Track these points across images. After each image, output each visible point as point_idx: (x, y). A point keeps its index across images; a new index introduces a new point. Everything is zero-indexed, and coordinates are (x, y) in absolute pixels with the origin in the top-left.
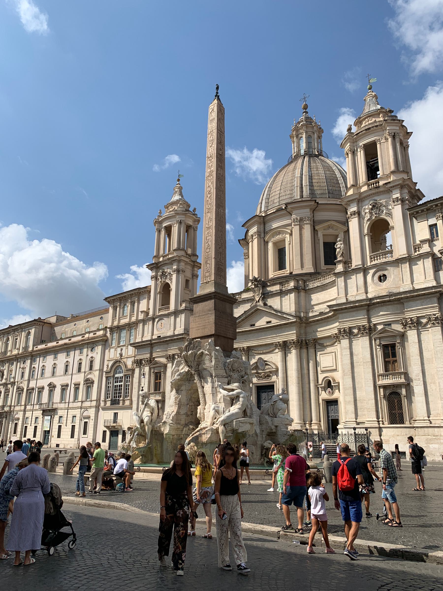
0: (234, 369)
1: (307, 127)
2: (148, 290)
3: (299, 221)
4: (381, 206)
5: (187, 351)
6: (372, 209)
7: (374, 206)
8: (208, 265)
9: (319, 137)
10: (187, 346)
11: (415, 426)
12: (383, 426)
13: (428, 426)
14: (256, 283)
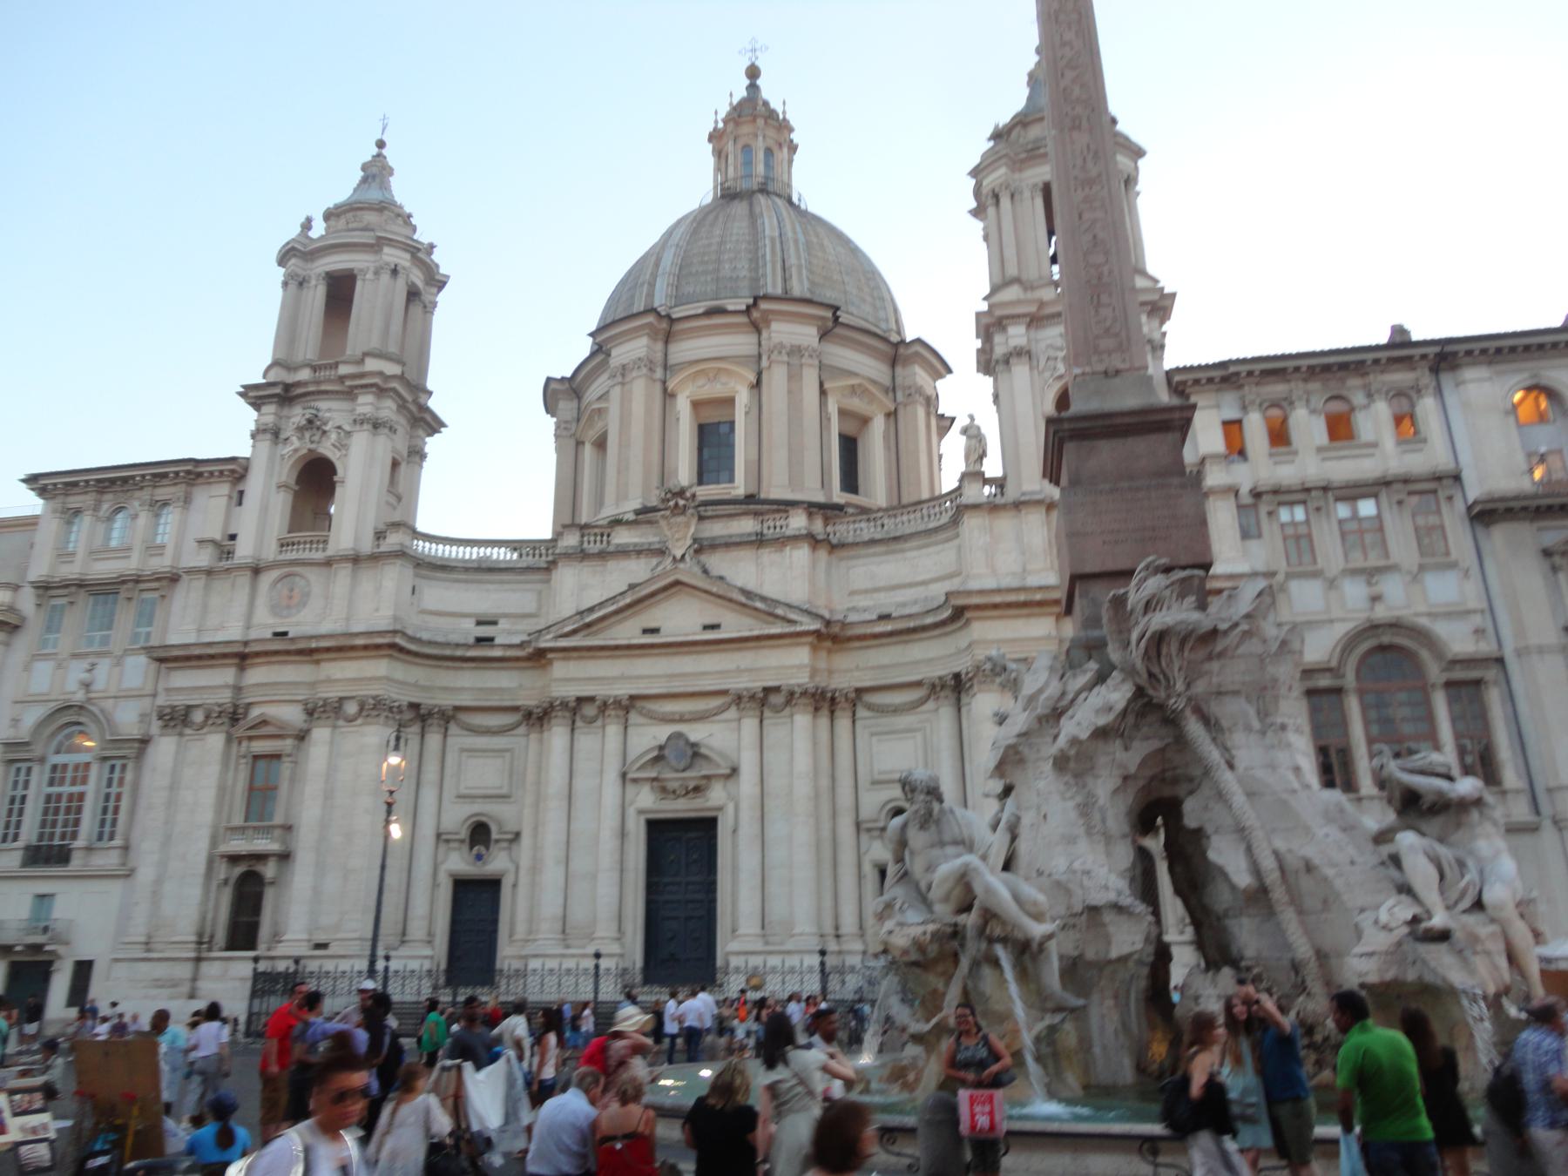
1: (766, 123)
2: (233, 471)
3: (788, 354)
8: (1105, 312)
9: (790, 162)
14: (681, 502)
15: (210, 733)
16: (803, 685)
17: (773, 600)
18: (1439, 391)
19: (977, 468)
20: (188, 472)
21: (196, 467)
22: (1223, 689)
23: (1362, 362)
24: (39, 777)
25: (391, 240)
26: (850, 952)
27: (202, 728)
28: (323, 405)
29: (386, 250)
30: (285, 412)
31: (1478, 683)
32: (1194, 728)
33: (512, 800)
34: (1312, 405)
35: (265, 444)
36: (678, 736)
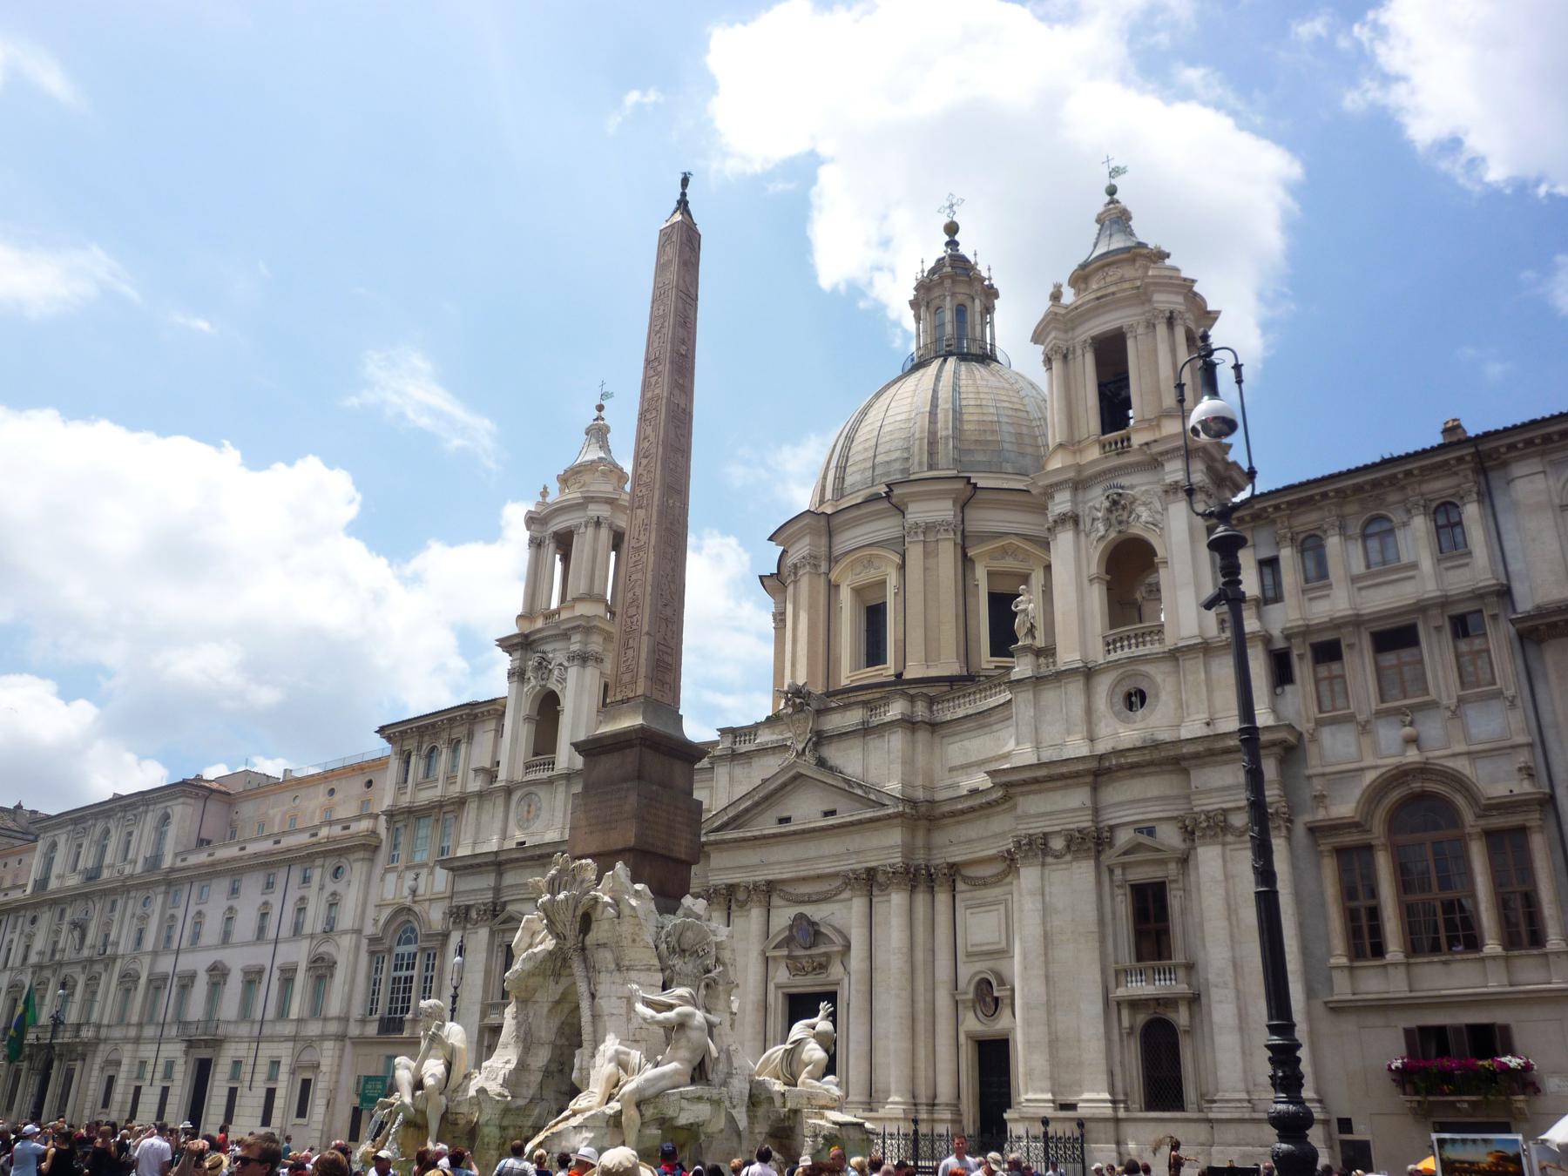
0: (686, 947)
1: (954, 282)
2: (496, 710)
3: (924, 533)
4: (1132, 503)
5: (553, 893)
6: (1109, 510)
7: (1115, 503)
8: (630, 652)
9: (989, 309)
10: (553, 879)
11: (1211, 1115)
12: (1122, 1114)
13: (1247, 1116)
14: (798, 701)
15: (481, 927)
16: (894, 865)
18: (1486, 497)
19: (1028, 641)
20: (468, 715)
21: (472, 709)
22: (600, 942)
23: (1394, 476)
24: (388, 965)
25: (593, 497)
26: (942, 1121)
27: (477, 923)
28: (548, 648)
29: (591, 506)
30: (530, 654)
31: (1523, 830)
32: (577, 967)
34: (1349, 533)
35: (515, 684)
36: (801, 916)
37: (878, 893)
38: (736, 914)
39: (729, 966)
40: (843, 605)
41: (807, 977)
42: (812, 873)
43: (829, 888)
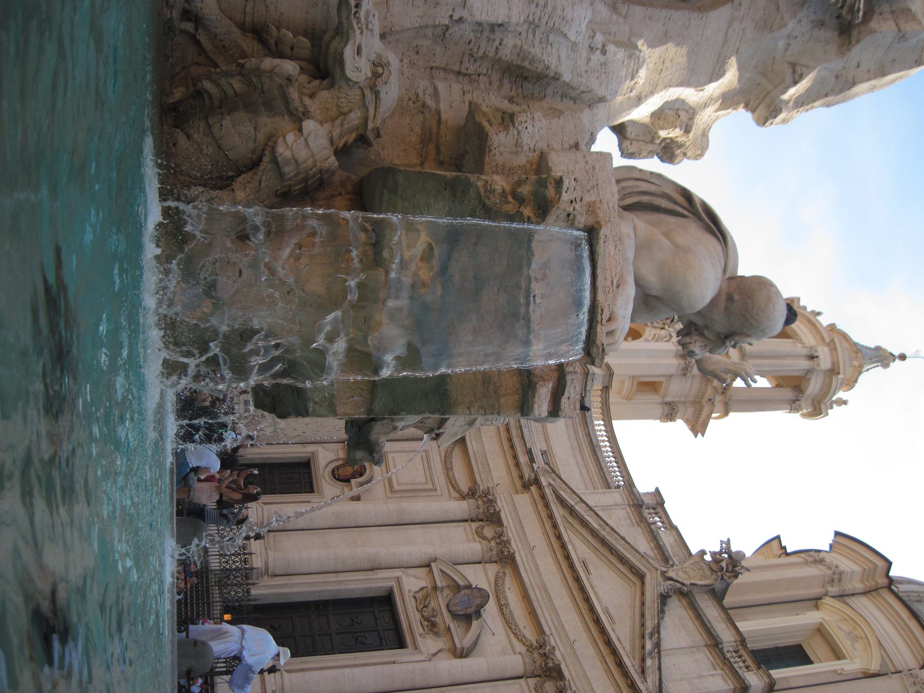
14: (724, 564)
17: (659, 652)
25: (835, 349)
29: (826, 349)
33: (389, 495)
37: (532, 686)
38: (468, 529)
39: (837, 64)
40: (801, 616)
41: (416, 612)
42: (536, 604)
43: (521, 627)
